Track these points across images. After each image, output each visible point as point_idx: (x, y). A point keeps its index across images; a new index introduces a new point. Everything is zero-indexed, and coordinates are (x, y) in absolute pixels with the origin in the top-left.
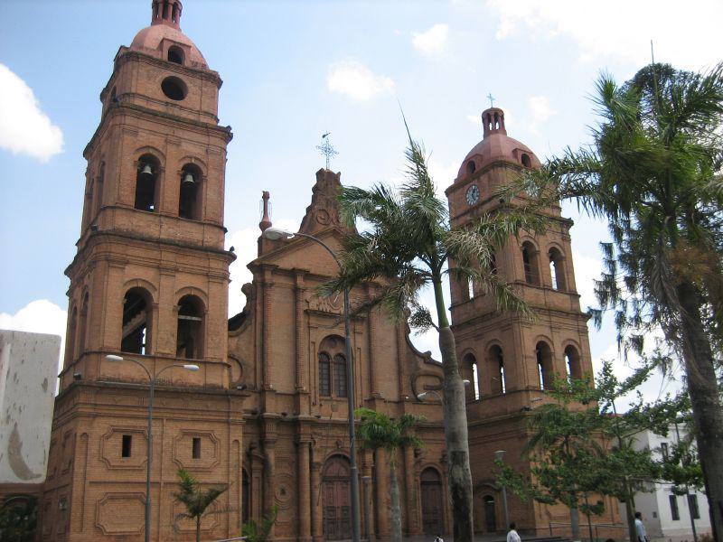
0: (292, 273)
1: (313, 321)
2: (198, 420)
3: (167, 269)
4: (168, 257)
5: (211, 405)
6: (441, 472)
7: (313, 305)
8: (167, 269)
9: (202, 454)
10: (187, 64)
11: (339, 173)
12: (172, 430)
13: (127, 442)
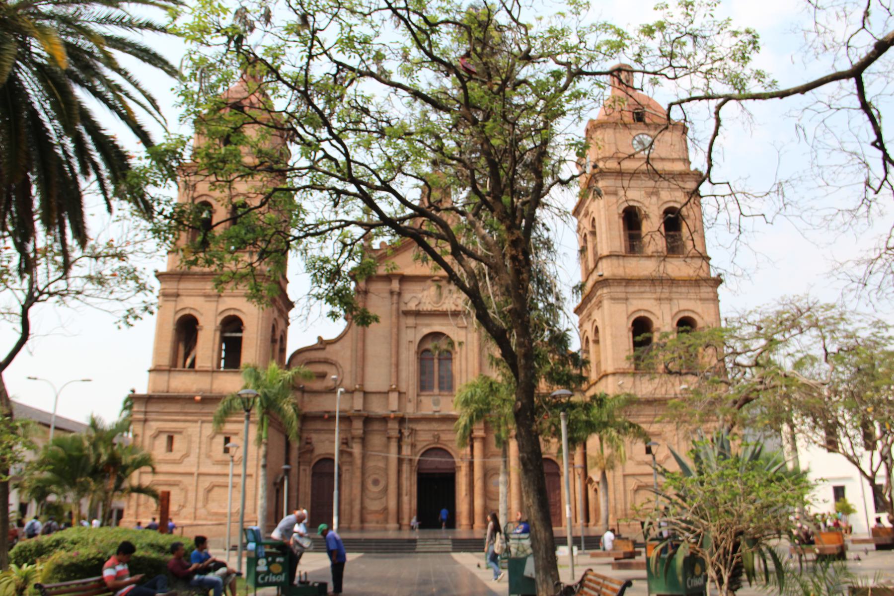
0: (388, 278)
1: (411, 321)
7: (412, 306)
13: (171, 439)
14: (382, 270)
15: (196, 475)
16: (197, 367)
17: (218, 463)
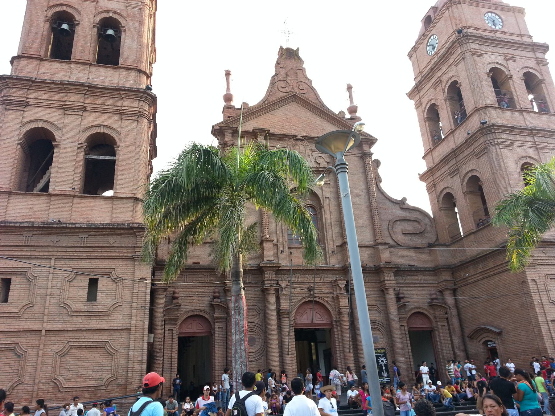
0: (253, 134)
2: (96, 258)
4: (75, 99)
6: (432, 318)
8: (72, 109)
9: (99, 295)
11: (298, 49)
14: (249, 126)
15: (43, 332)
16: (51, 191)
17: (78, 314)
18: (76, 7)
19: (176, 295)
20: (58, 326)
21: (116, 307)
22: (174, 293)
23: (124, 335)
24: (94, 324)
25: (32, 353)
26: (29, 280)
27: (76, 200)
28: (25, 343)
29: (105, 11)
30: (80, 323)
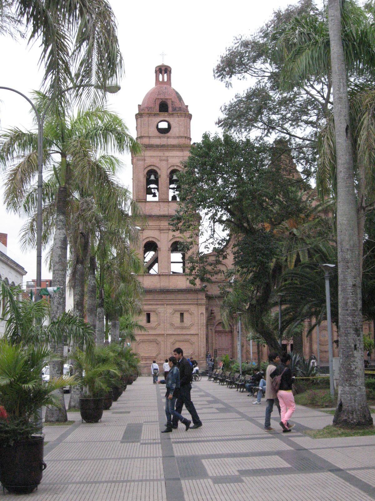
3: (163, 230)
5: (188, 296)
8: (163, 230)
9: (185, 320)
10: (170, 109)
12: (170, 309)
17: (178, 328)
18: (157, 166)
19: (213, 312)
20: (170, 332)
21: (192, 325)
22: (212, 310)
23: (196, 337)
24: (184, 332)
25: (162, 343)
26: (157, 314)
27: (171, 277)
28: (159, 339)
29: (172, 166)
30: (178, 332)
